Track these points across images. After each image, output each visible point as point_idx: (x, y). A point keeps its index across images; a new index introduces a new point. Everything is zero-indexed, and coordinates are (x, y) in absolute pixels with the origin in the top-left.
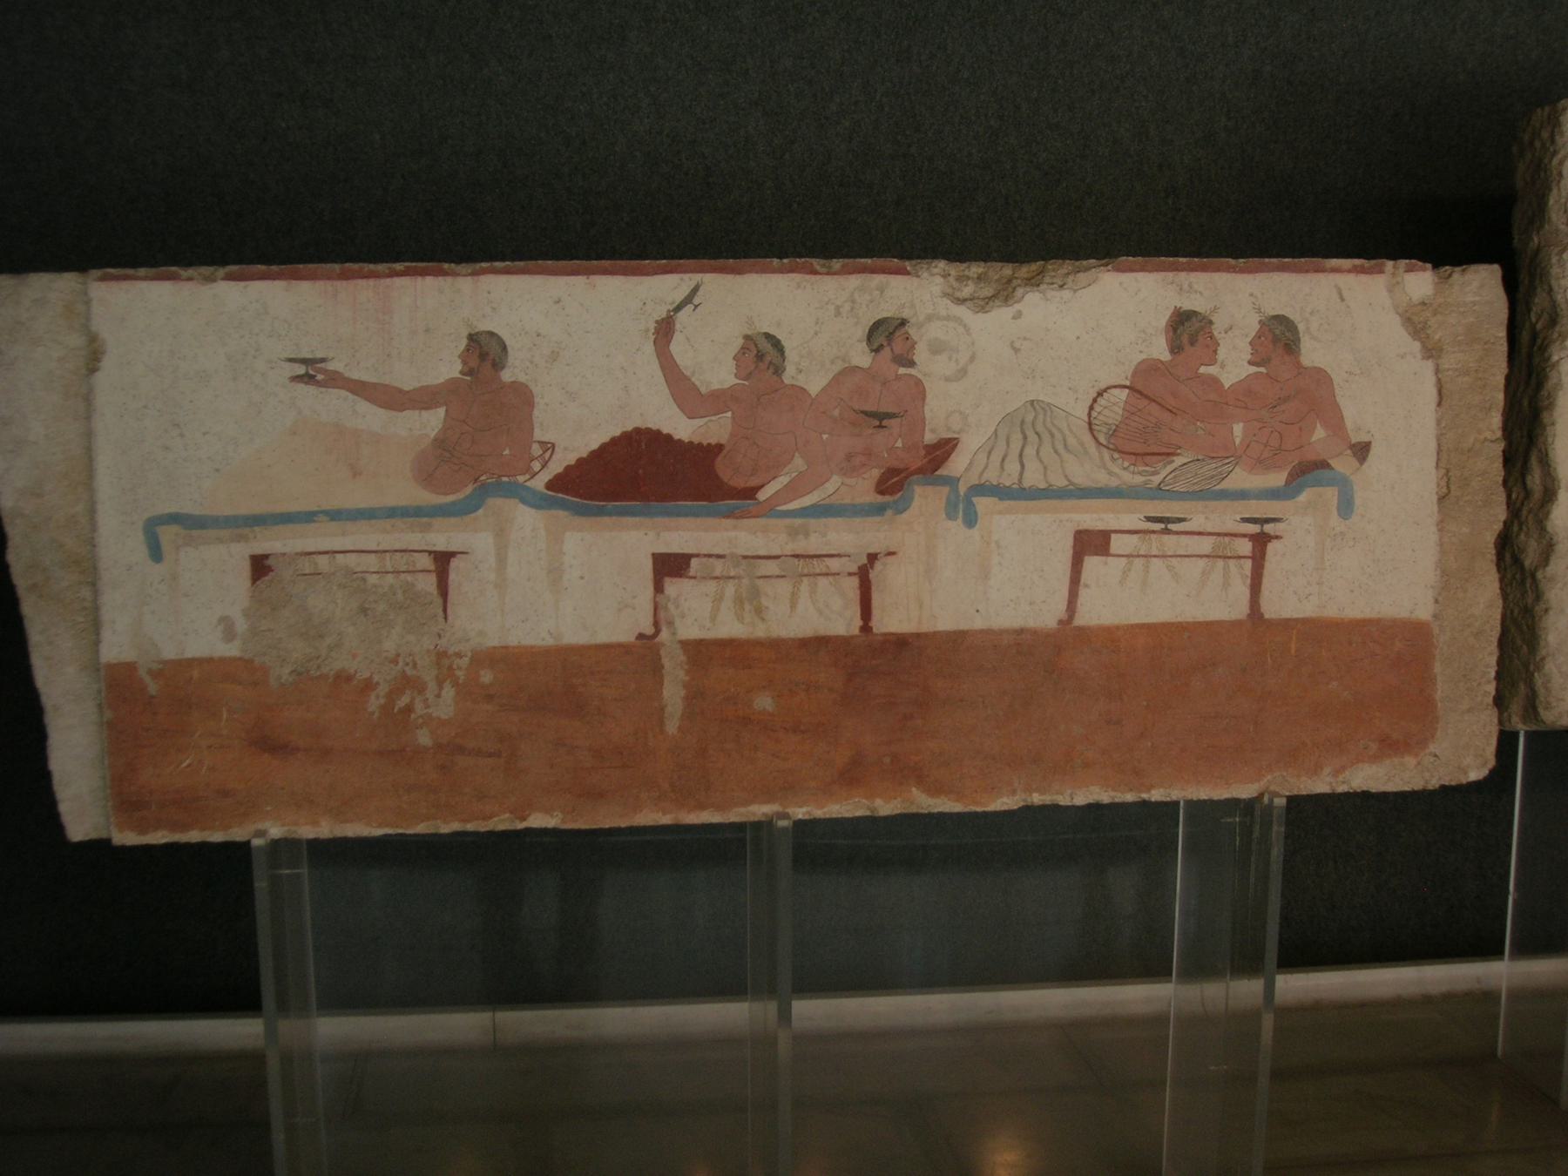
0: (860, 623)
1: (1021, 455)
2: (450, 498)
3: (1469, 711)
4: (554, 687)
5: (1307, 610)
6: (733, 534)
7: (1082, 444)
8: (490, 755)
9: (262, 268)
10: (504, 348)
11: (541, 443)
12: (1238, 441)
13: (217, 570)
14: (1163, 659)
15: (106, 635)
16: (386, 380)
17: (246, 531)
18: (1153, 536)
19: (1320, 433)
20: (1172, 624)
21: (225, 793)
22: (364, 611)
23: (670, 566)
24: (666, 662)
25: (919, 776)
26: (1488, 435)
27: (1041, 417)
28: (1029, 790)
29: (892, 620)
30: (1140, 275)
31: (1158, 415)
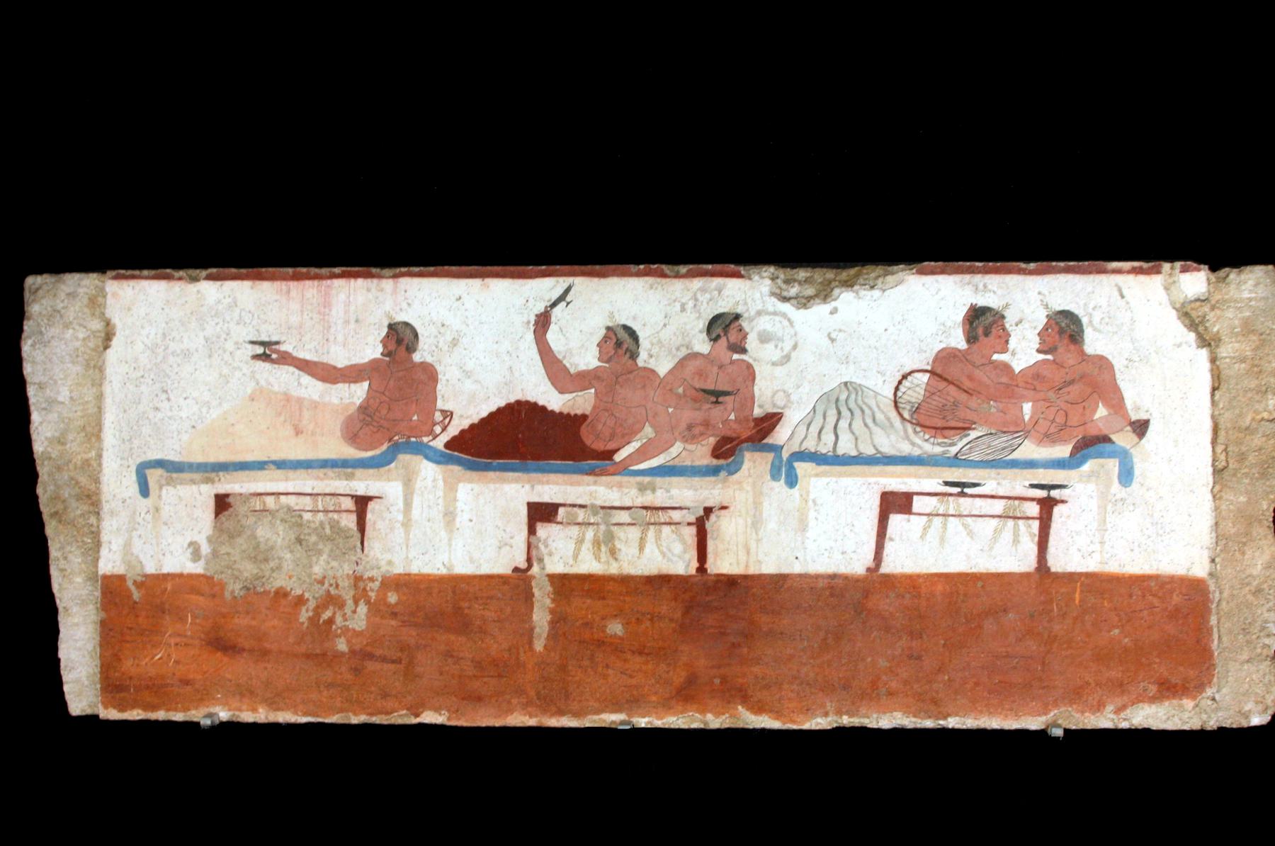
0: (695, 564)
1: (835, 427)
2: (370, 454)
3: (1248, 661)
4: (444, 609)
5: (1091, 565)
6: (593, 488)
7: (888, 419)
8: (393, 662)
9: (233, 270)
10: (416, 335)
11: (442, 411)
12: (1027, 418)
13: (189, 507)
14: (959, 604)
15: (104, 552)
16: (325, 359)
17: (213, 475)
18: (951, 499)
19: (1102, 412)
20: (967, 574)
21: (186, 682)
22: (299, 541)
23: (541, 513)
24: (536, 591)
25: (745, 699)
26: (1265, 415)
27: (853, 396)
28: (839, 713)
29: (724, 563)
30: (941, 278)
31: (956, 394)
